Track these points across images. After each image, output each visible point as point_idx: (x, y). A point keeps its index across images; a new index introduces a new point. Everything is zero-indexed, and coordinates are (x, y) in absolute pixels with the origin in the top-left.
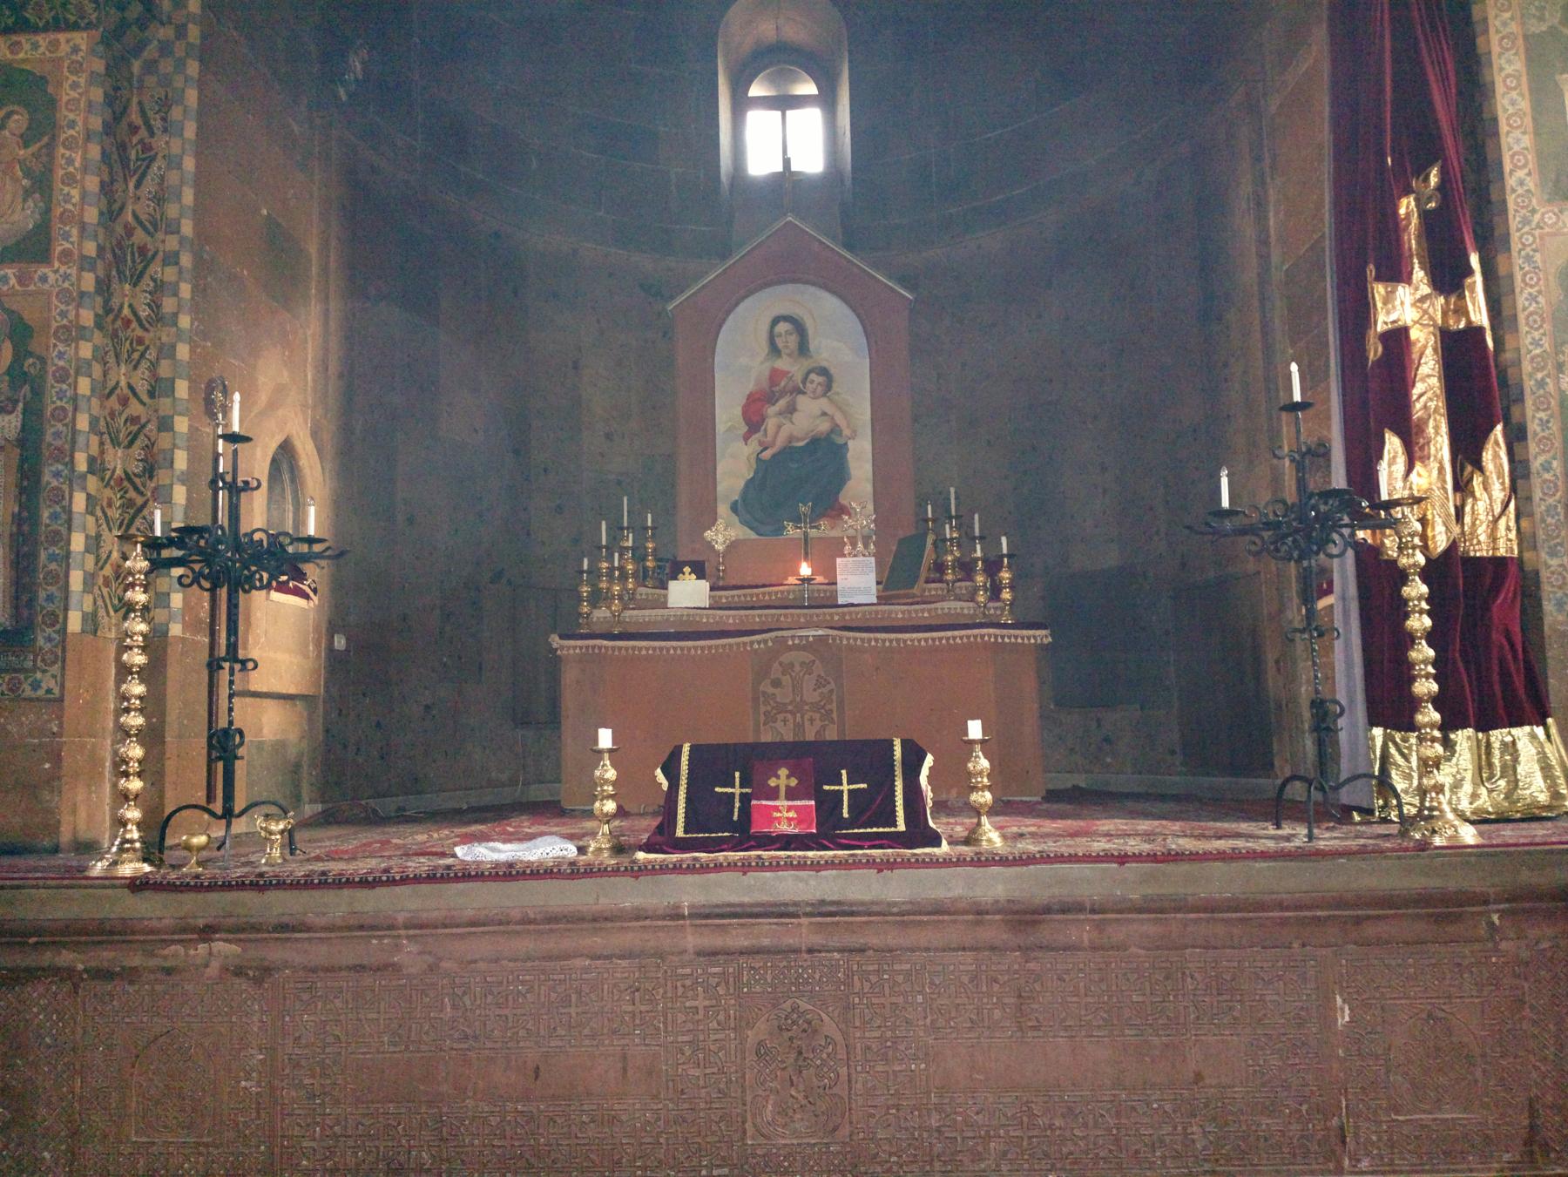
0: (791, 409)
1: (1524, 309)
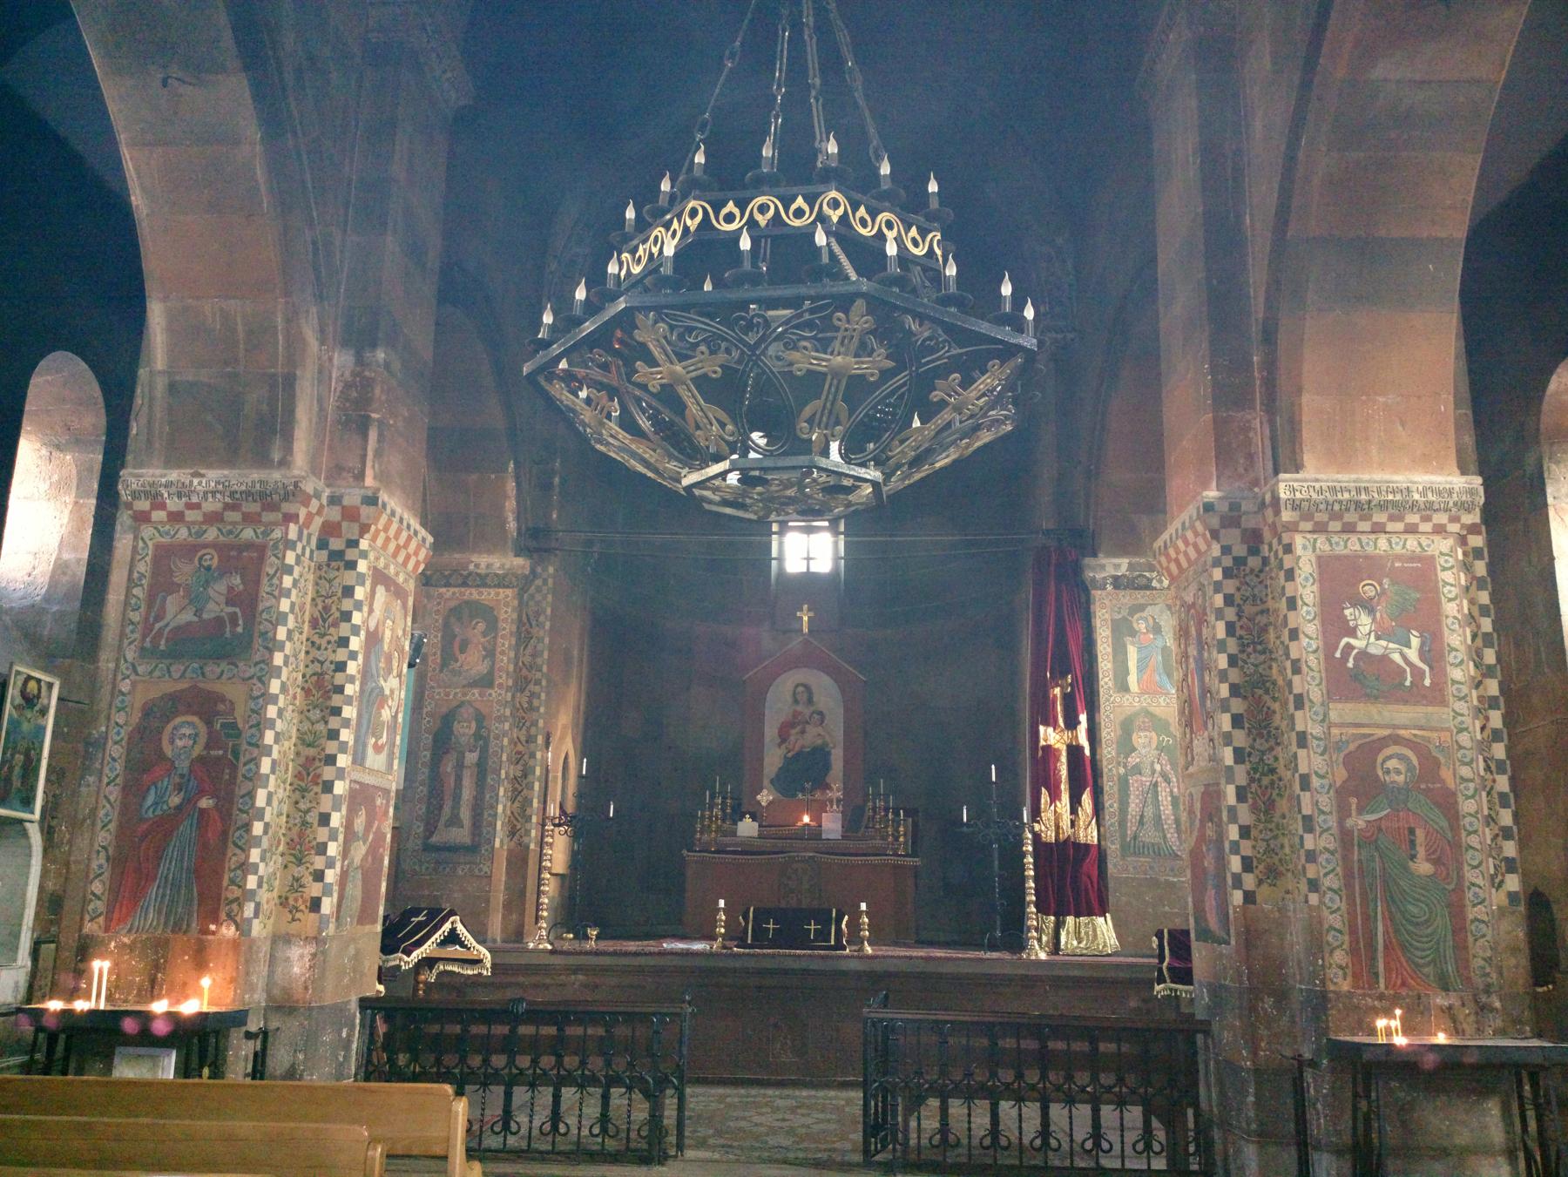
0: (803, 732)
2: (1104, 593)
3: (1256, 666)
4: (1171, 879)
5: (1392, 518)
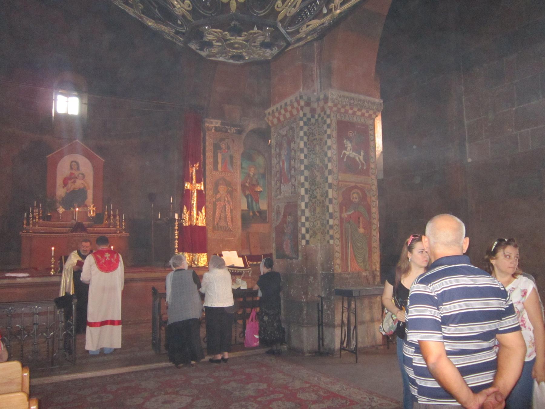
0: (75, 182)
3: (312, 159)
4: (229, 239)
5: (359, 110)
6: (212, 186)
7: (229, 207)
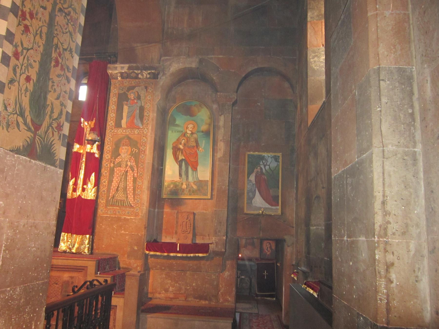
1: (107, 149)
2: (117, 81)
4: (127, 217)
6: (110, 148)
7: (132, 174)
